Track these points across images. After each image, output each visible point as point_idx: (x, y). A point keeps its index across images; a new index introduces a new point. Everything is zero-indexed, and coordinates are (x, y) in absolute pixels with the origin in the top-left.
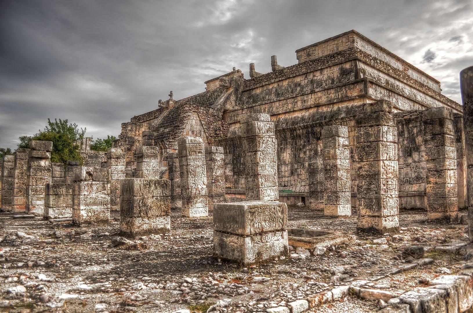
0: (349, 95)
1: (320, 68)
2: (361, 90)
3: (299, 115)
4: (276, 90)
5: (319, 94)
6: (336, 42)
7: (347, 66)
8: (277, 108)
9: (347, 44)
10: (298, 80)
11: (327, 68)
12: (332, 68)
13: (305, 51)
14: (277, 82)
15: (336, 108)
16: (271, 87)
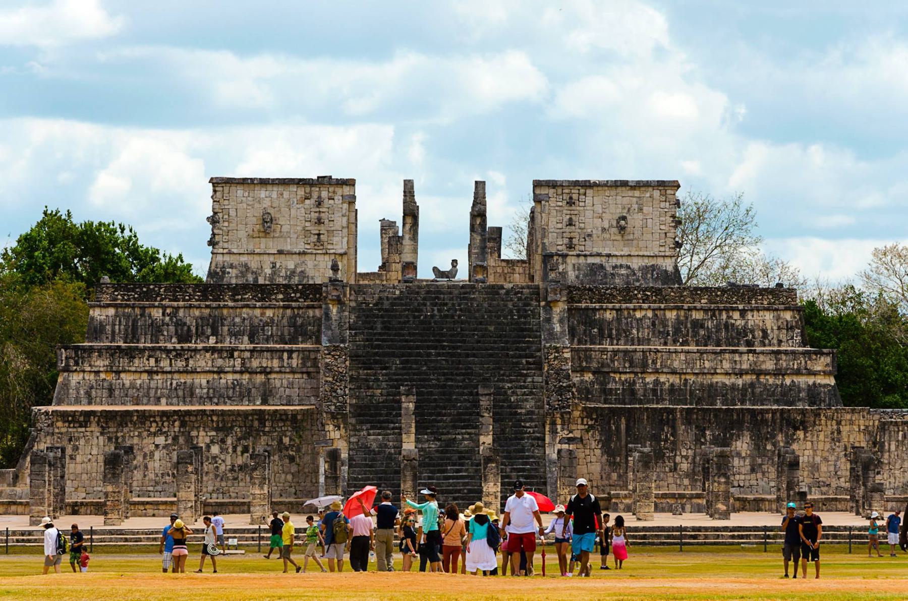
1: (741, 307)
2: (827, 365)
3: (727, 381)
4: (654, 324)
5: (762, 358)
6: (637, 193)
9: (662, 205)
11: (752, 310)
12: (761, 313)
13: (560, 191)
14: (654, 310)
15: (788, 381)
16: (638, 315)
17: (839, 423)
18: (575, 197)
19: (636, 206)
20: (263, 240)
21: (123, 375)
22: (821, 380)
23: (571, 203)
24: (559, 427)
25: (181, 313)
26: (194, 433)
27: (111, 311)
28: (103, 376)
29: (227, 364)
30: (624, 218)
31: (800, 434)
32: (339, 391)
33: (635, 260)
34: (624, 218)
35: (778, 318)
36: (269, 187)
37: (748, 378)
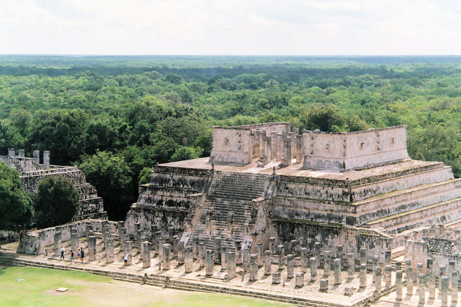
0: (348, 210)
5: (332, 205)
7: (346, 190)
8: (308, 205)
10: (318, 188)
16: (301, 186)
17: (348, 233)
18: (314, 137)
19: (332, 141)
20: (226, 147)
21: (155, 196)
22: (352, 215)
23: (313, 139)
24: (249, 230)
25: (174, 176)
26: (167, 217)
27: (157, 175)
28: (150, 196)
29: (181, 195)
30: (327, 145)
31: (336, 235)
32: (193, 212)
33: (332, 159)
34: (327, 145)
35: (343, 191)
36: (227, 130)
37: (329, 212)
